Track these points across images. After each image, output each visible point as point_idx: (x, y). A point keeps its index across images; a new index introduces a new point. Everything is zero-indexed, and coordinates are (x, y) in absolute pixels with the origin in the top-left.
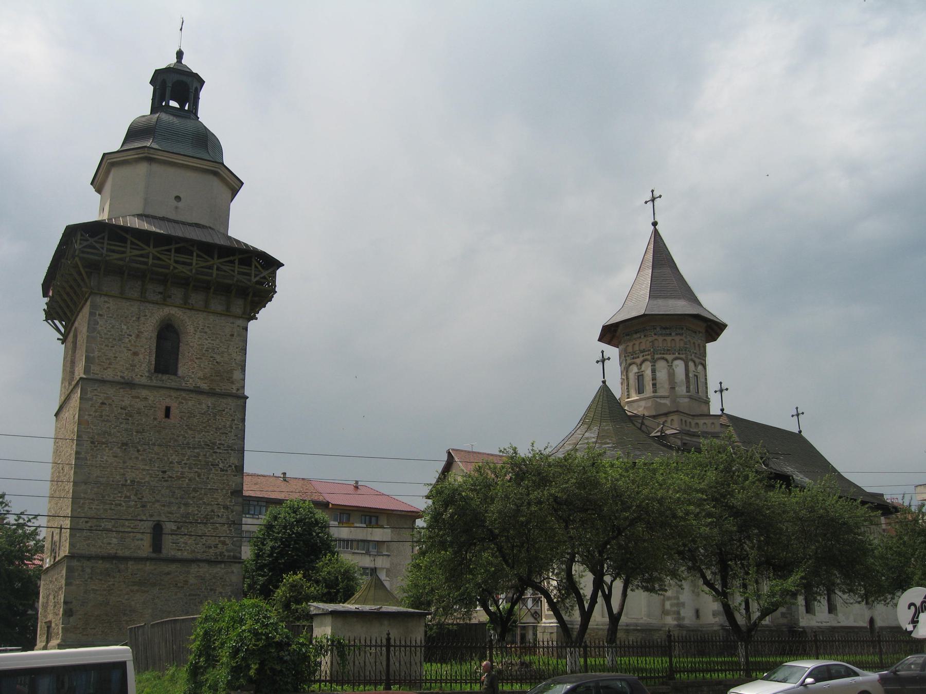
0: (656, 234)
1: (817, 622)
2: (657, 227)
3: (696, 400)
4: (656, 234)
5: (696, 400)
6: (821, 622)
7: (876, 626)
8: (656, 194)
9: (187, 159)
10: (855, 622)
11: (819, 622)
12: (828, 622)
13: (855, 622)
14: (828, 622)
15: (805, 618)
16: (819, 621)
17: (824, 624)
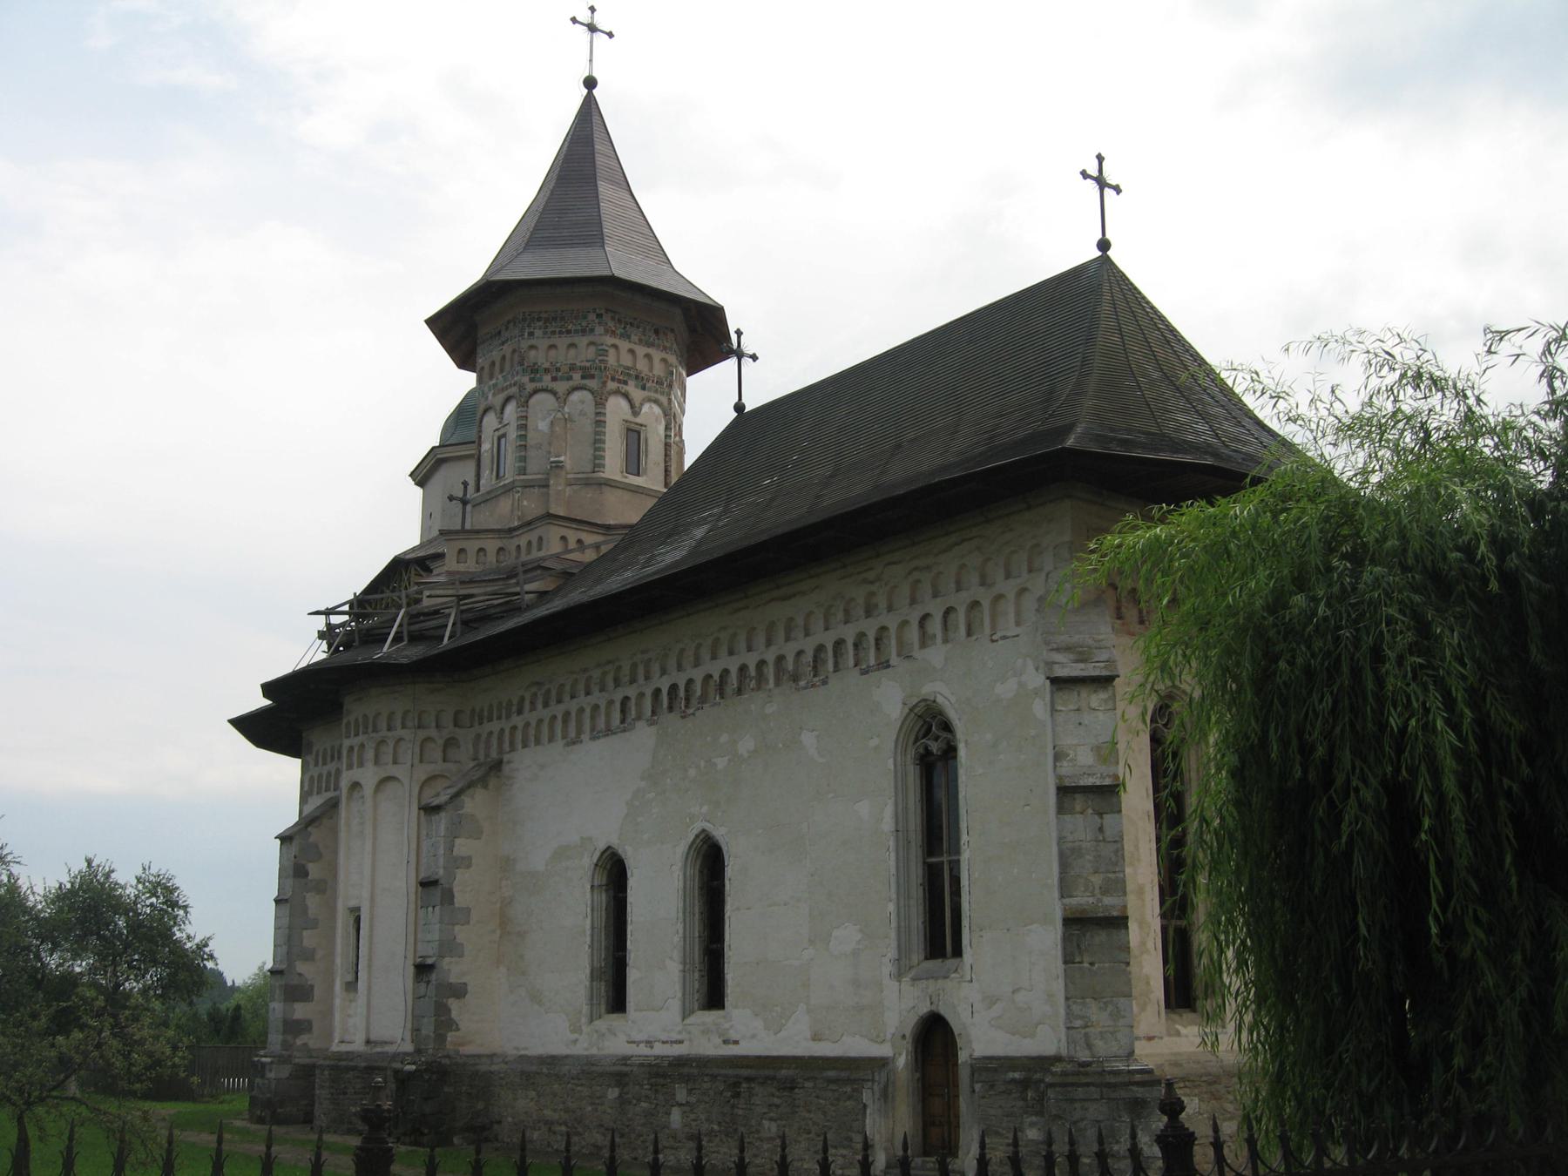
0: (589, 115)
1: (629, 1042)
2: (595, 91)
3: (487, 500)
4: (589, 115)
5: (487, 500)
6: (649, 1043)
7: (963, 1056)
8: (584, 16)
9: (464, 447)
10: (816, 1037)
11: (638, 1043)
12: (681, 1042)
13: (816, 1037)
14: (681, 1042)
15: (585, 1029)
16: (638, 1037)
17: (659, 1050)
